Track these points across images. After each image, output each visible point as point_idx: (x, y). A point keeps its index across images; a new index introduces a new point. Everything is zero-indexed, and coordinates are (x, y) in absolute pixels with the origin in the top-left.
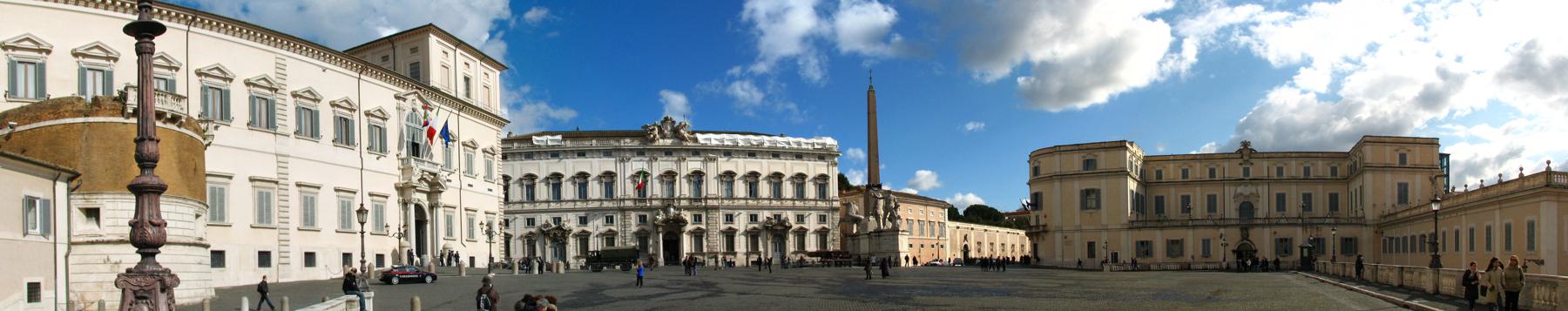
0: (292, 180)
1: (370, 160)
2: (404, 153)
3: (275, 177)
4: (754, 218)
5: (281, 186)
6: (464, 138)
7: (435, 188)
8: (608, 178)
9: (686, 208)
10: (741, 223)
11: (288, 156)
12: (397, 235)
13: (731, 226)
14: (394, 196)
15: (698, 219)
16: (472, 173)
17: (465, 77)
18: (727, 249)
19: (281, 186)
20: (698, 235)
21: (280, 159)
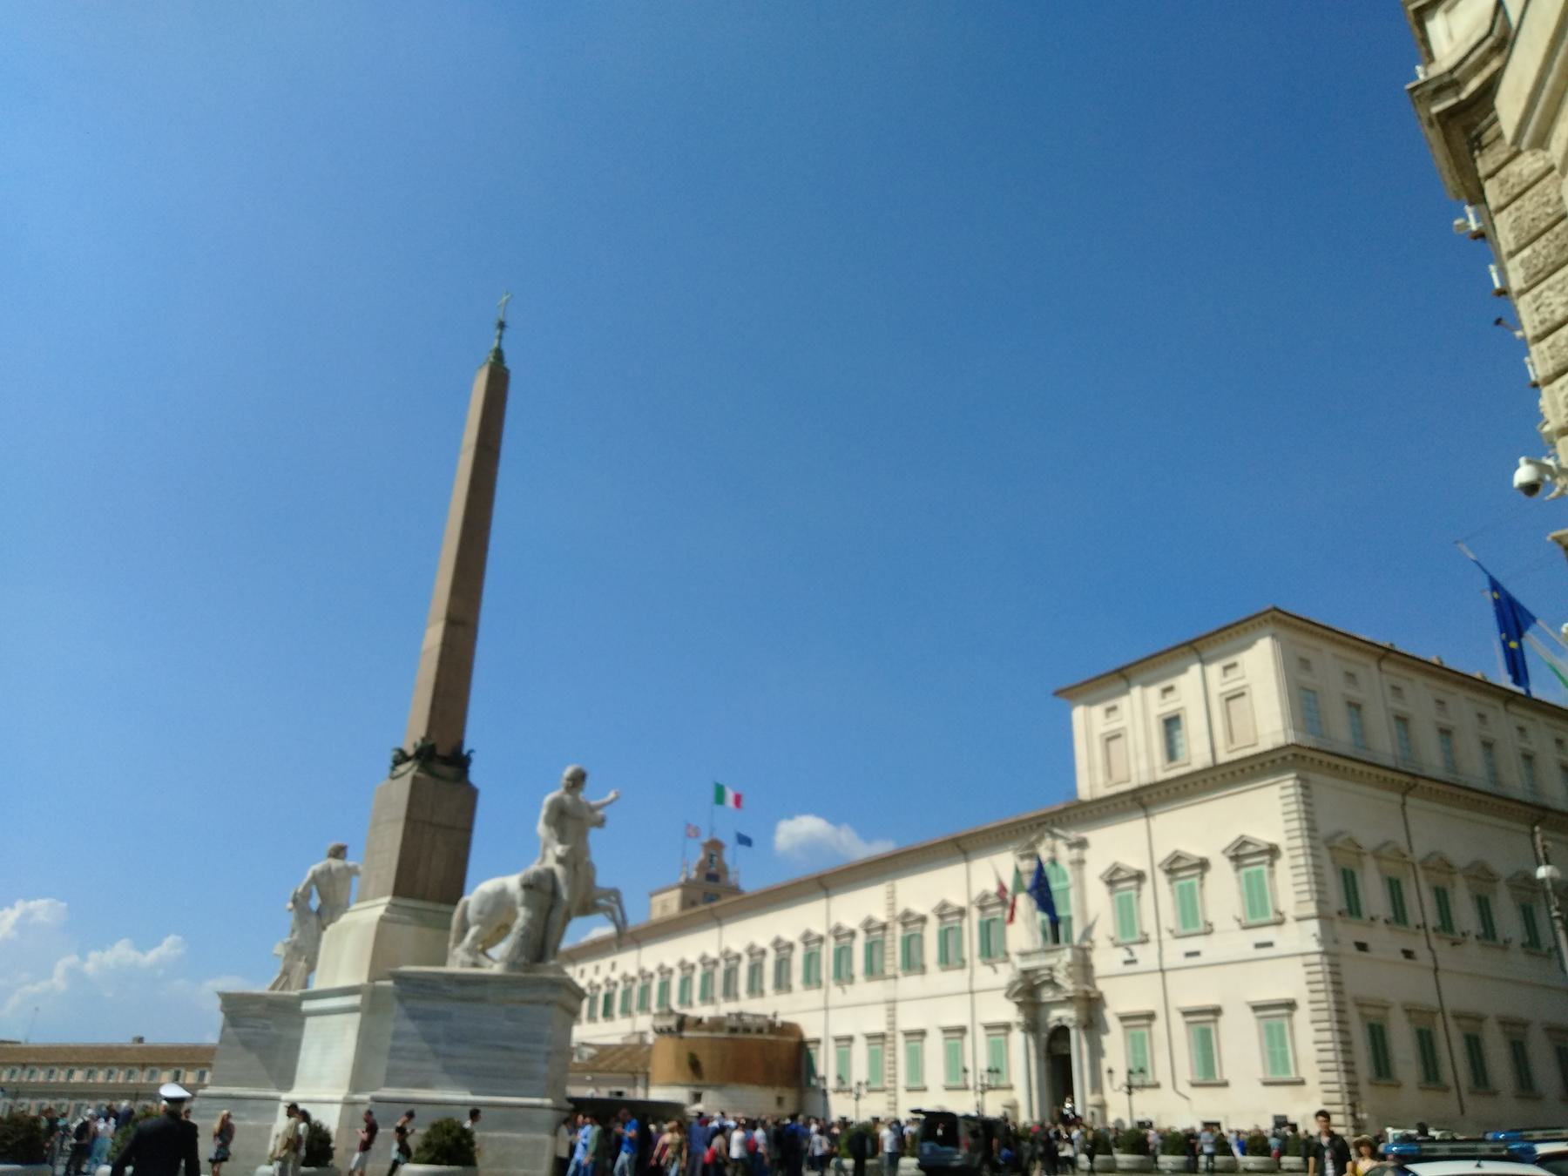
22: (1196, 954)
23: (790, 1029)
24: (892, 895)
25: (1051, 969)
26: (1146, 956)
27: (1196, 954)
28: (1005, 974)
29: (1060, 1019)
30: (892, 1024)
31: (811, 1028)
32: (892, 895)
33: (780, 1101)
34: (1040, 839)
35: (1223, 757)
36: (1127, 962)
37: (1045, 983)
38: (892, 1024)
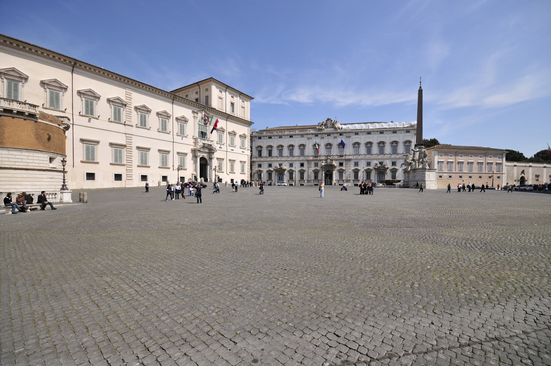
0: (134, 145)
1: (178, 139)
2: (197, 135)
3: (124, 143)
4: (369, 164)
5: (128, 147)
6: (230, 130)
7: (211, 150)
8: (302, 147)
9: (337, 160)
10: (362, 167)
11: (133, 135)
13: (357, 168)
14: (190, 155)
15: (341, 164)
16: (233, 145)
17: (231, 103)
18: (355, 178)
19: (128, 147)
20: (341, 172)
21: (127, 135)
22: (233, 150)
26: (224, 147)
27: (233, 150)
35: (240, 118)
36: (220, 148)
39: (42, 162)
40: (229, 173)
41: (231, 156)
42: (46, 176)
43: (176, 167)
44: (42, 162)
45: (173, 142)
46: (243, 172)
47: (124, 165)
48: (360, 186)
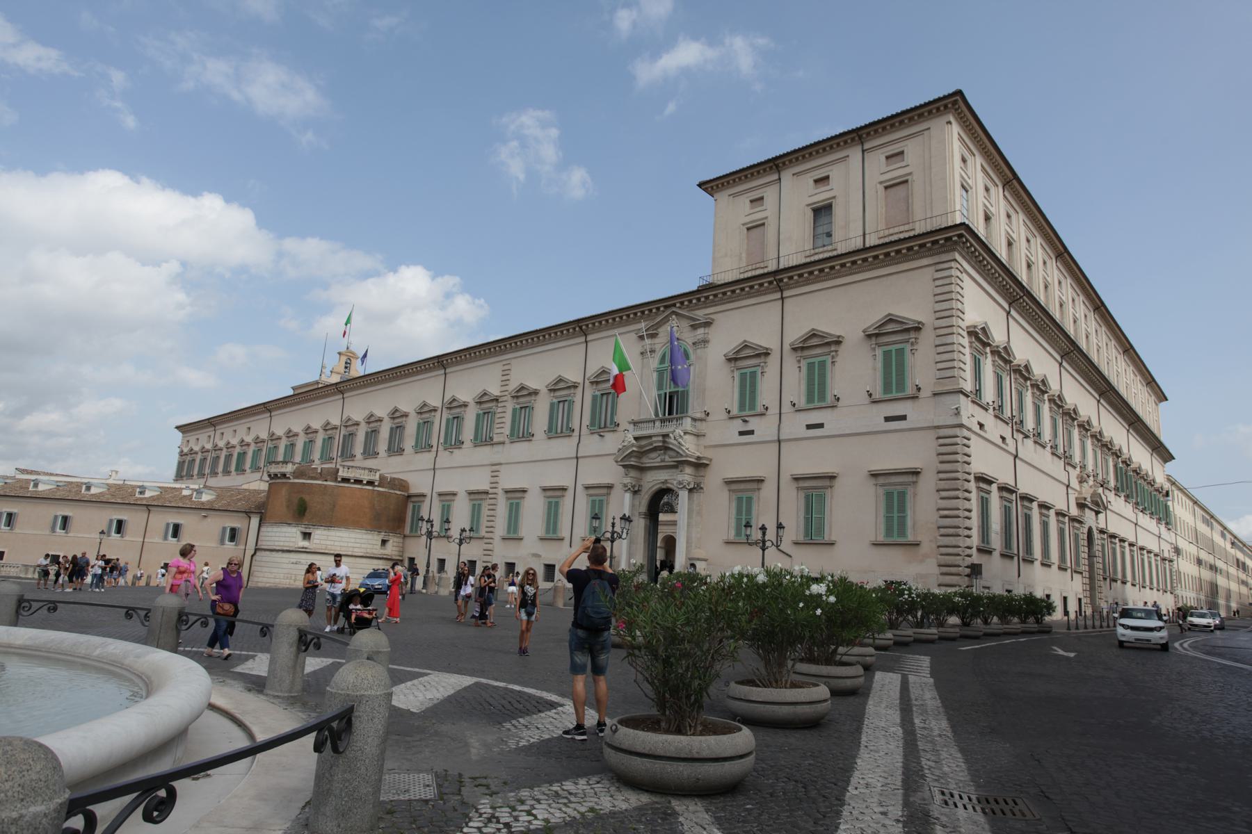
1: (592, 444)
3: (485, 486)
11: (500, 464)
12: (457, 541)
19: (490, 496)
21: (495, 468)
22: (821, 426)
23: (402, 485)
24: (506, 373)
25: (666, 436)
26: (764, 428)
27: (821, 426)
28: (613, 443)
29: (666, 482)
30: (494, 484)
31: (419, 483)
32: (506, 373)
33: (384, 542)
34: (665, 320)
35: (872, 241)
36: (741, 433)
37: (655, 449)
38: (494, 484)
39: (288, 539)
40: (796, 543)
41: (804, 461)
42: (287, 561)
43: (455, 533)
44: (288, 539)
45: (577, 458)
46: (551, 535)
47: (482, 538)
48: (648, 646)
